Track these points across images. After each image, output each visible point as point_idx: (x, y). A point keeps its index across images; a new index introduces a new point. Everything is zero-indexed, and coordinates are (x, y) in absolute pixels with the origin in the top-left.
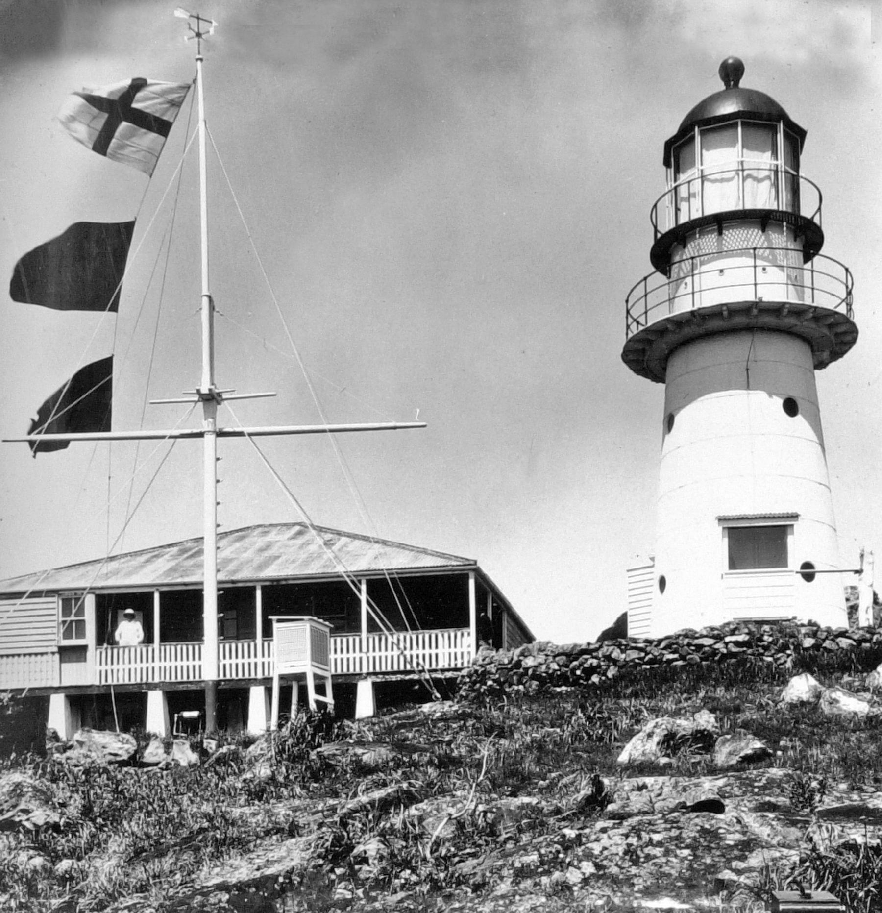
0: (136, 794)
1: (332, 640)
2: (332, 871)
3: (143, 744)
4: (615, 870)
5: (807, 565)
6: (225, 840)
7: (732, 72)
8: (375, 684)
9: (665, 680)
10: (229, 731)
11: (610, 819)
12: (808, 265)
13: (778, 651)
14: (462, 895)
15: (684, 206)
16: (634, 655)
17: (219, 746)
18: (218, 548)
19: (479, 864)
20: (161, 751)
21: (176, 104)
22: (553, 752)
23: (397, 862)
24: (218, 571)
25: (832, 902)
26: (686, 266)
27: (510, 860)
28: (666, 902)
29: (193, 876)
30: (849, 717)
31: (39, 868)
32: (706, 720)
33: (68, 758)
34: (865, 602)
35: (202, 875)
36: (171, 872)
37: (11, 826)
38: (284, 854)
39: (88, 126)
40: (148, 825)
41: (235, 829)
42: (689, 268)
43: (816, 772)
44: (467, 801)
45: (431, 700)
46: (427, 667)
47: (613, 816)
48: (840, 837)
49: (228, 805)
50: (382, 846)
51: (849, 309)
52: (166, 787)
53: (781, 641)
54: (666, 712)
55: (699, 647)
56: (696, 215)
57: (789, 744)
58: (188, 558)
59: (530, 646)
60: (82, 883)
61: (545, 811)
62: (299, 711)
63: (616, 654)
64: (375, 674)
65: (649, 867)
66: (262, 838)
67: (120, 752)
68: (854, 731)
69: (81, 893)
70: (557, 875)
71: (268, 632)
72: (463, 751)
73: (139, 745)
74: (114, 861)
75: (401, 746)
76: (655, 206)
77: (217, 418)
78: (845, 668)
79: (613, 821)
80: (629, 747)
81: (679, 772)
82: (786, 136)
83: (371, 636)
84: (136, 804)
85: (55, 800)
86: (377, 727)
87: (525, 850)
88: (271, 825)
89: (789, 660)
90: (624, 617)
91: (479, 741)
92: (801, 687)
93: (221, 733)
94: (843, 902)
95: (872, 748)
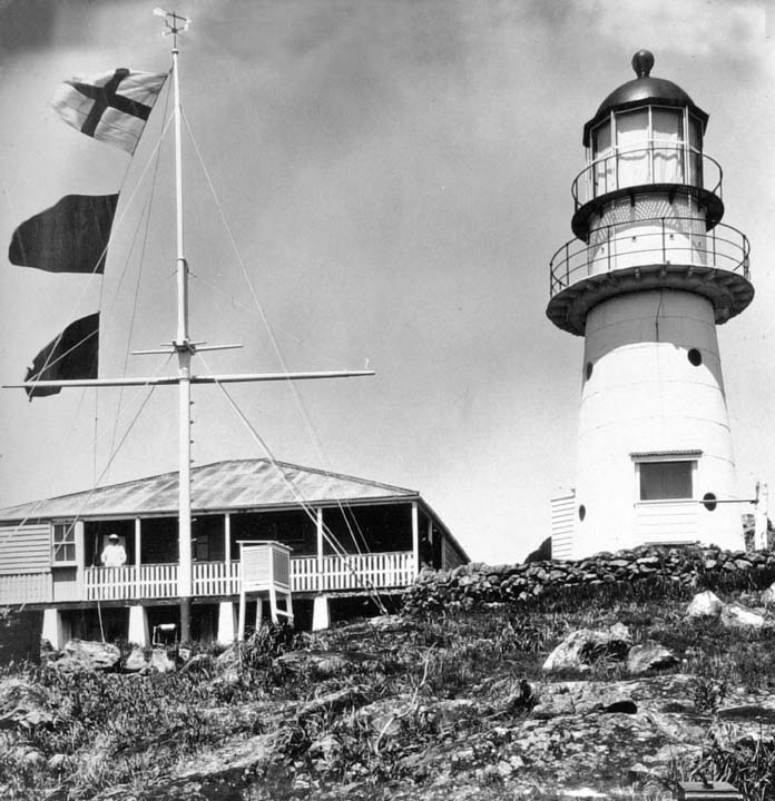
0: (120, 697)
1: (292, 562)
2: (292, 764)
3: (126, 653)
4: (540, 764)
5: (710, 496)
6: (198, 737)
7: (643, 63)
8: (329, 600)
9: (585, 597)
10: (202, 641)
11: (536, 718)
12: (710, 233)
13: (684, 572)
14: (406, 785)
15: (601, 181)
16: (557, 575)
17: (193, 655)
18: (191, 481)
19: (421, 759)
20: (142, 659)
21: (155, 92)
22: (486, 660)
23: (348, 757)
24: (192, 501)
25: (731, 792)
26: (603, 234)
27: (448, 755)
28: (585, 792)
29: (170, 769)
30: (746, 629)
31: (34, 762)
32: (620, 632)
33: (60, 665)
34: (760, 529)
35: (178, 768)
36: (150, 765)
37: (9, 725)
38: (250, 749)
39: (78, 110)
40: (130, 724)
41: (207, 728)
42: (606, 235)
43: (717, 677)
44: (410, 703)
45: (379, 615)
46: (375, 585)
47: (539, 716)
48: (739, 734)
49: (201, 707)
50: (336, 743)
51: (747, 272)
52: (146, 690)
53: (686, 562)
54: (586, 625)
55: (615, 568)
56: (612, 189)
57: (694, 653)
58: (165, 489)
59: (466, 567)
60: (72, 775)
61: (479, 712)
62: (262, 624)
63: (542, 574)
64: (330, 591)
65: (570, 761)
66: (230, 736)
67: (106, 660)
68: (751, 642)
69: (71, 783)
70: (489, 768)
71: (235, 555)
72: (407, 659)
73: (122, 653)
74: (100, 756)
75: (352, 655)
76: (576, 181)
77: (192, 367)
78: (743, 586)
79: (538, 721)
80: (552, 655)
81: (597, 678)
82: (691, 119)
83: (326, 558)
84: (119, 706)
85: (48, 702)
86: (331, 638)
87: (462, 746)
88: (238, 724)
89: (694, 579)
90: (549, 539)
91: (421, 650)
92: (704, 603)
93: (195, 643)
94: (741, 792)
95: (766, 657)
